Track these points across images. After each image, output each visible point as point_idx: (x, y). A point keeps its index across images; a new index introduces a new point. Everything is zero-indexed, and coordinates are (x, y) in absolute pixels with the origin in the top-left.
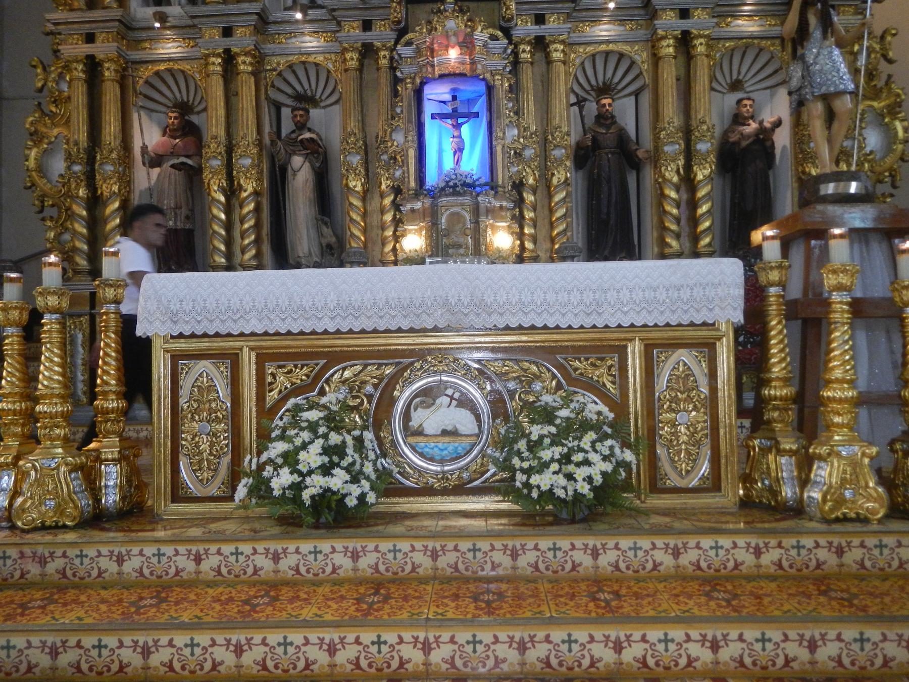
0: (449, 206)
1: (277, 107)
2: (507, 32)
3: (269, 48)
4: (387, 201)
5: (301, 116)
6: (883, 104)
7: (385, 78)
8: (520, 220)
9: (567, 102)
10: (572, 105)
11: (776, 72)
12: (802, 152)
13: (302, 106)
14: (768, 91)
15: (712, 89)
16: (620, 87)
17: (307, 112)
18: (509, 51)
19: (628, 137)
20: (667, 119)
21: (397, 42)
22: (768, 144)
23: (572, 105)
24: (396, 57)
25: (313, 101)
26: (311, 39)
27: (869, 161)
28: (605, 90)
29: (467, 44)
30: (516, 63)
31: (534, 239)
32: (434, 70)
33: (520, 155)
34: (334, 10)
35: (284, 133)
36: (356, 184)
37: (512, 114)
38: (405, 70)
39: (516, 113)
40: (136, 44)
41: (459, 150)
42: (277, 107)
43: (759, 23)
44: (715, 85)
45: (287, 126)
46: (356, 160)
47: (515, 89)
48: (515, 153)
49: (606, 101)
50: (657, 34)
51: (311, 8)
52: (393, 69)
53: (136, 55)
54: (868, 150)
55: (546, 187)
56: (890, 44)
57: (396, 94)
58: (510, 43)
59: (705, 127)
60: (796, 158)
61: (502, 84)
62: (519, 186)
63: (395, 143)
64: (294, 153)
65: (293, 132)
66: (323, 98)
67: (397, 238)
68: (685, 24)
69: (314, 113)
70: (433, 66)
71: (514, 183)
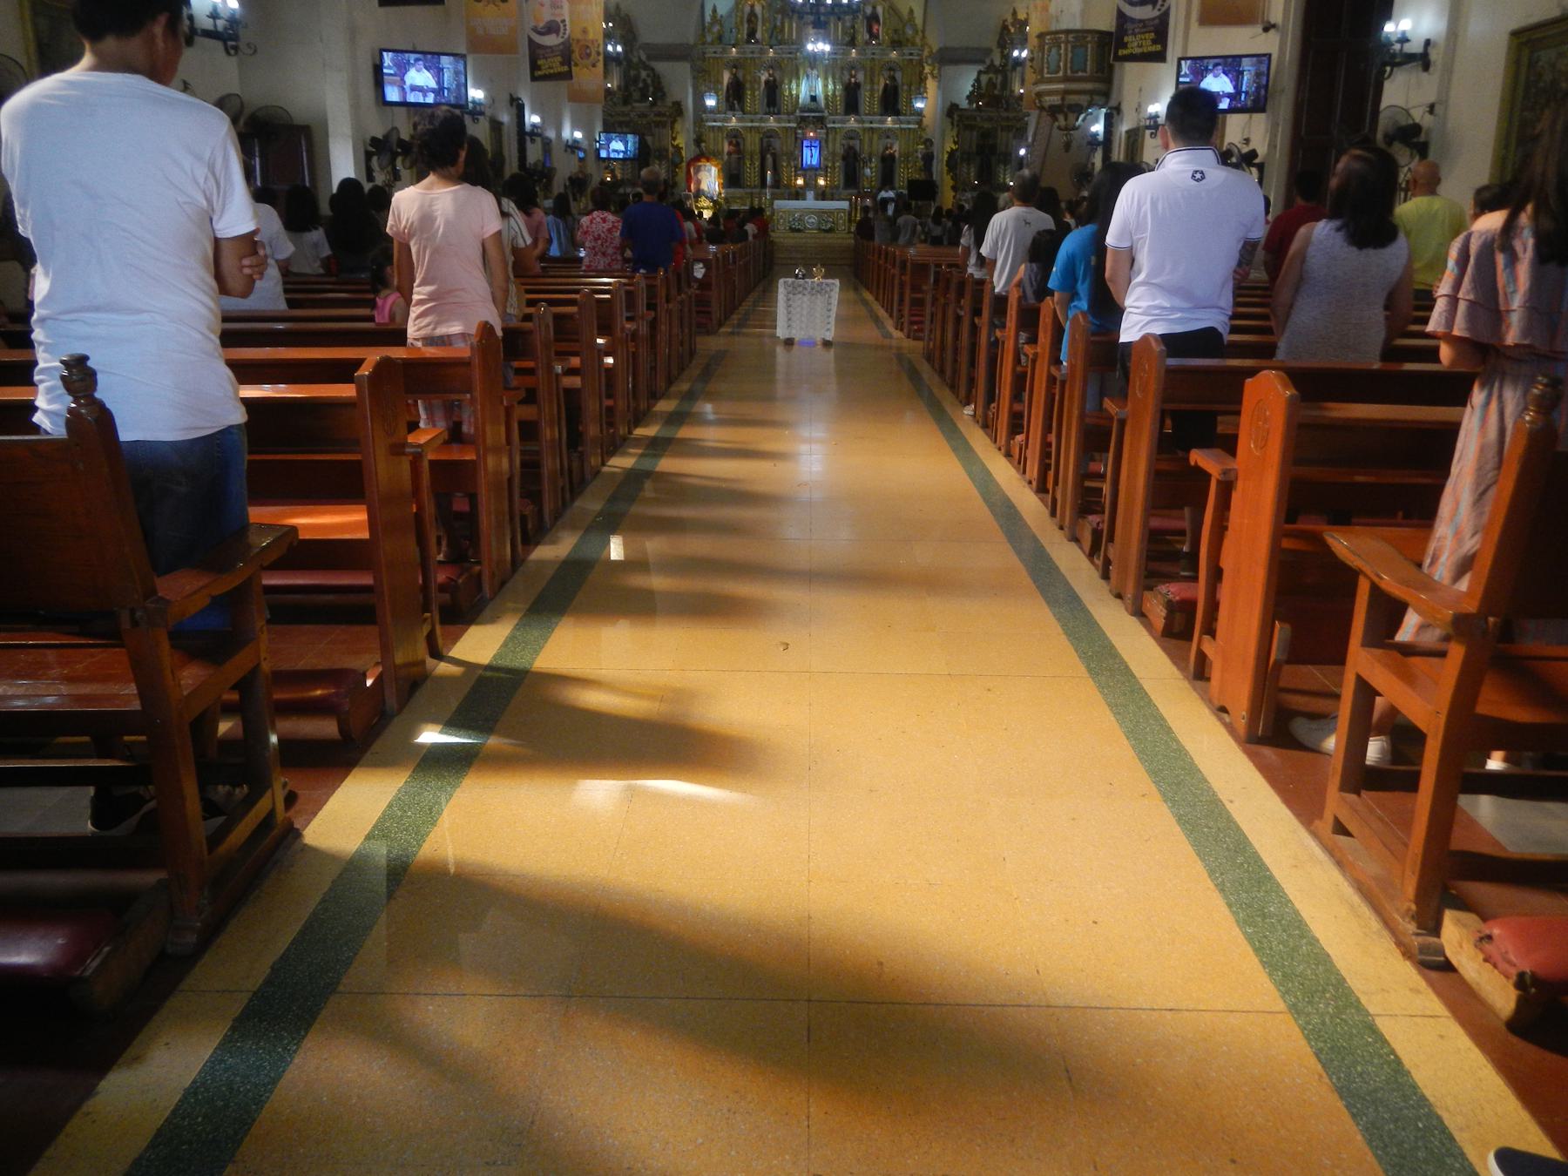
0: (809, 173)
3: (763, 125)
4: (793, 169)
7: (793, 135)
8: (826, 176)
25: (771, 137)
28: (851, 138)
29: (815, 132)
30: (827, 134)
31: (830, 181)
36: (785, 164)
41: (812, 156)
45: (765, 145)
46: (785, 158)
47: (827, 141)
53: (726, 124)
55: (833, 168)
61: (823, 144)
62: (827, 167)
67: (796, 180)
68: (872, 125)
69: (772, 139)
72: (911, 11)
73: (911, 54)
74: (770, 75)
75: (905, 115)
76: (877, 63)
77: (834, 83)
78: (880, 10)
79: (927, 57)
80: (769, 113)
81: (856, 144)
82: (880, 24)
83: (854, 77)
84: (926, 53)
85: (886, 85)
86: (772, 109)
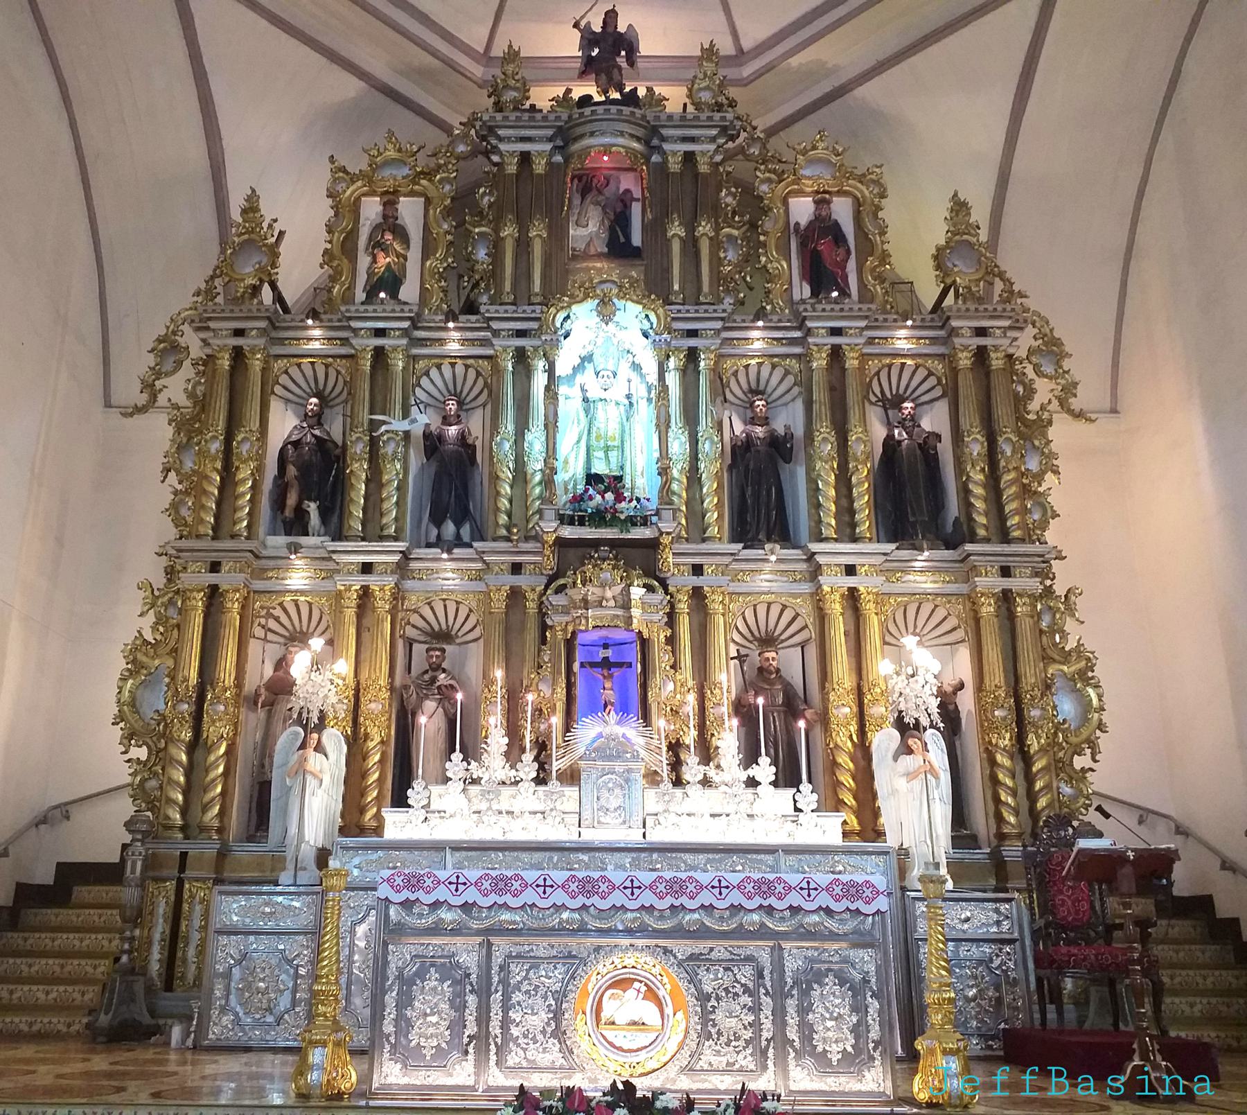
1: (410, 643)
2: (664, 584)
5: (437, 656)
6: (1073, 669)
9: (727, 654)
10: (732, 659)
11: (954, 629)
12: (987, 720)
13: (438, 646)
14: (949, 647)
15: (885, 643)
16: (783, 637)
17: (443, 651)
18: (665, 603)
19: (796, 694)
20: (835, 680)
21: (547, 587)
22: (951, 707)
23: (732, 659)
24: (546, 602)
26: (455, 576)
27: (1063, 731)
32: (587, 621)
33: (677, 712)
34: (484, 552)
35: (415, 671)
37: (668, 668)
38: (555, 620)
39: (673, 667)
40: (260, 574)
42: (410, 643)
43: (931, 578)
44: (888, 639)
47: (671, 641)
48: (672, 710)
49: (772, 655)
50: (822, 590)
51: (457, 546)
52: (542, 614)
54: (1060, 718)
56: (1075, 603)
57: (543, 641)
58: (667, 593)
59: (879, 691)
60: (982, 726)
63: (542, 694)
64: (427, 697)
65: (426, 672)
66: (460, 634)
69: (448, 648)
70: (587, 618)
71: (670, 742)
72: (959, 207)
73: (981, 332)
74: (446, 421)
75: (987, 540)
76: (852, 363)
77: (694, 441)
78: (842, 210)
79: (1031, 352)
80: (439, 543)
81: (789, 661)
82: (848, 252)
83: (765, 421)
84: (1026, 340)
85: (890, 444)
86: (449, 528)
